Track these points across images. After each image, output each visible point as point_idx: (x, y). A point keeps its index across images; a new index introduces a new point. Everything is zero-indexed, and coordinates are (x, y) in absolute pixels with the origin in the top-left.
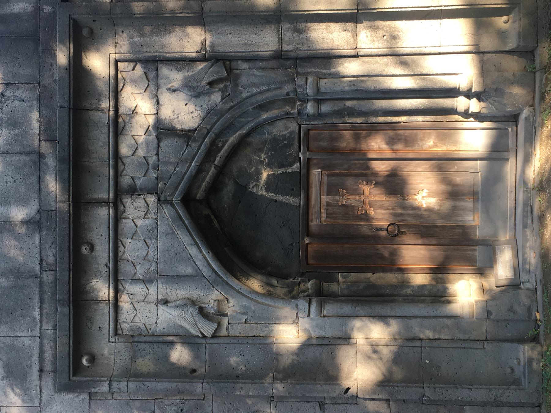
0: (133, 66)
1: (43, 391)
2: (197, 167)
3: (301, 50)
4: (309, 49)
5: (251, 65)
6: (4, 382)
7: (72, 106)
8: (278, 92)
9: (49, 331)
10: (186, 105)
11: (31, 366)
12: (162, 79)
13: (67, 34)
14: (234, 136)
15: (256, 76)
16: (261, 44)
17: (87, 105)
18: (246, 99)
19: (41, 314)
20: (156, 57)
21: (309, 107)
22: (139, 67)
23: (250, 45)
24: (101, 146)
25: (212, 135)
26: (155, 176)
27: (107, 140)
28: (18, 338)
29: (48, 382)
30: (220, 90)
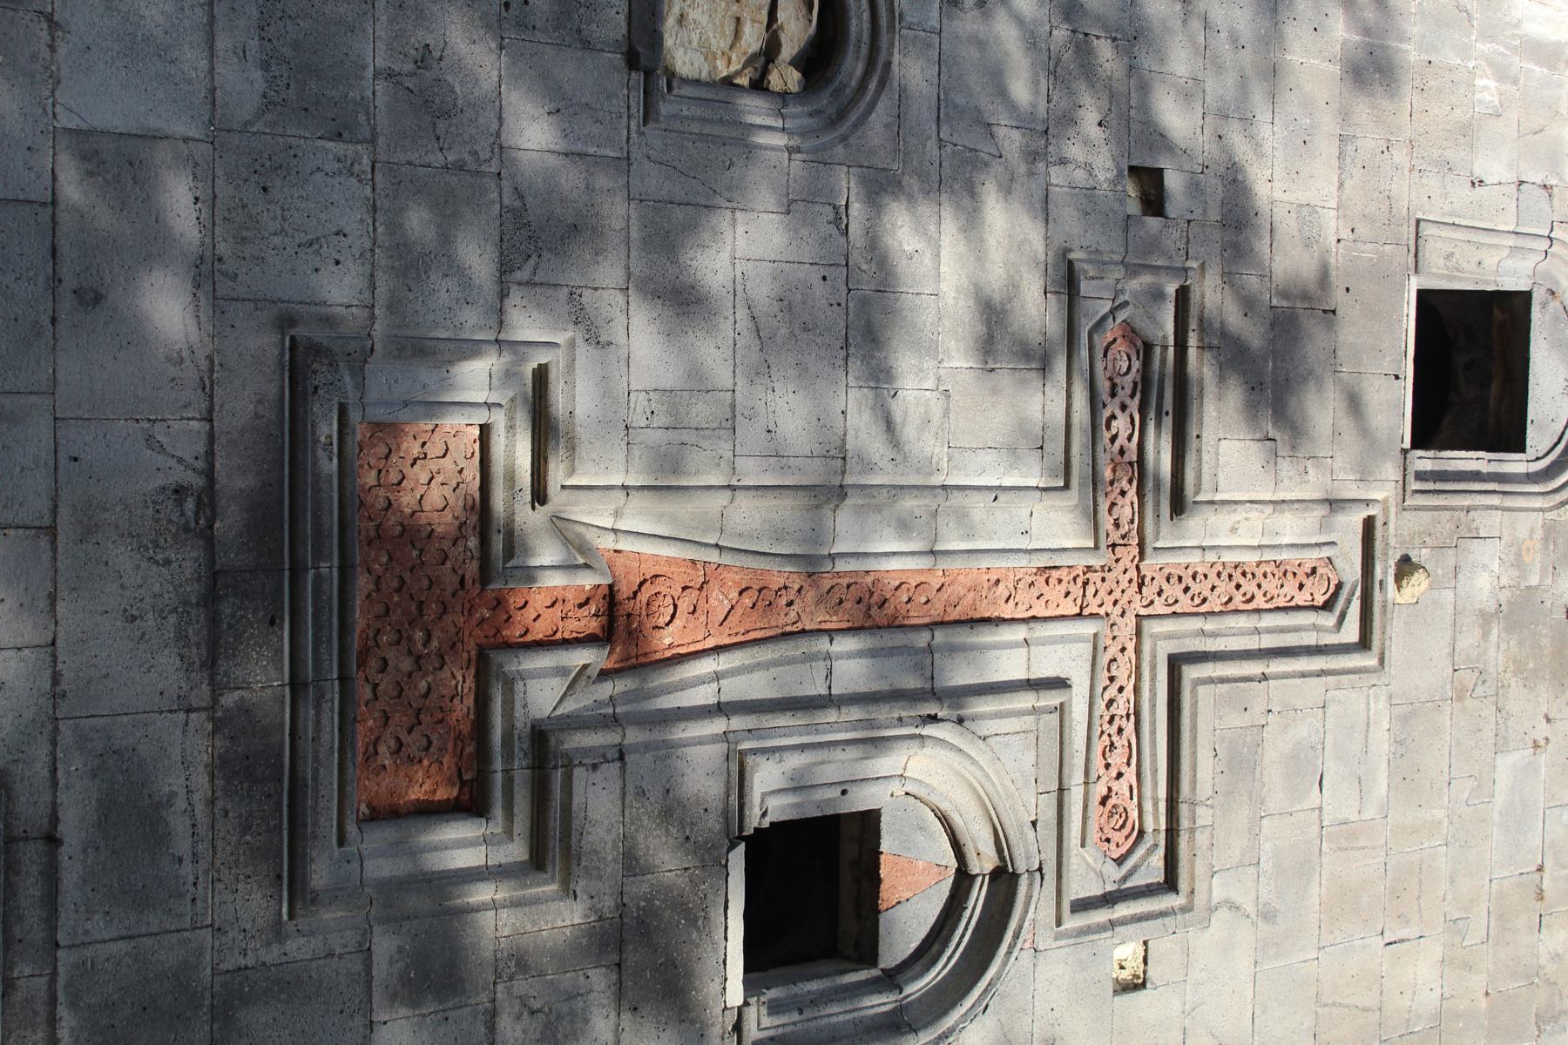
1: (45, 773)
6: (167, 789)
9: (27, 971)
11: (84, 851)
19: (52, 1021)
28: (124, 933)
29: (29, 807)
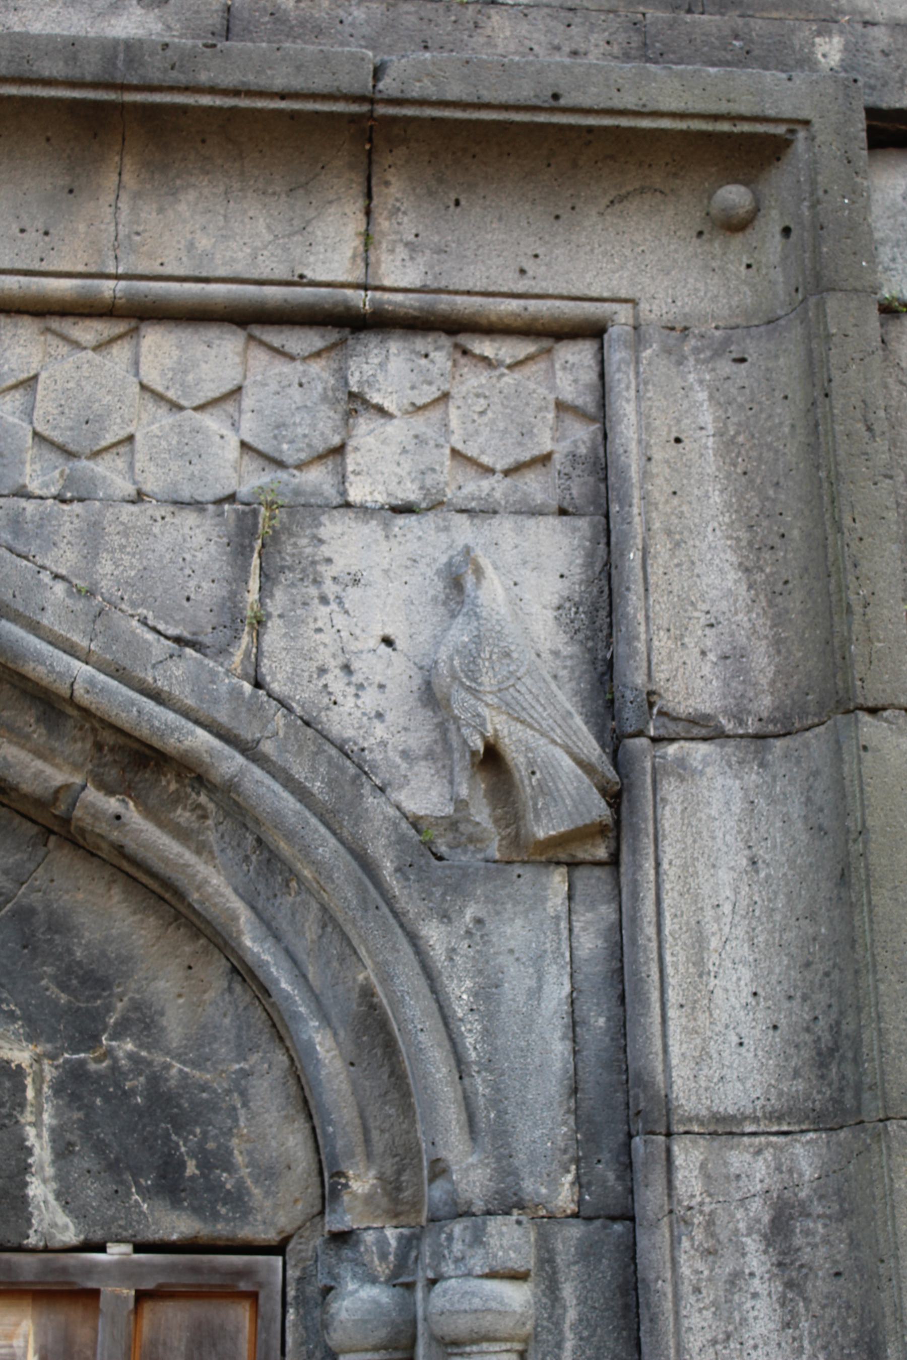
0: (579, 402)
2: (64, 691)
3: (675, 1242)
4: (686, 1288)
5: (594, 970)
7: (382, 110)
8: (451, 1115)
10: (388, 641)
12: (519, 531)
13: (723, 107)
14: (228, 892)
15: (536, 993)
16: (702, 1017)
17: (394, 190)
18: (413, 939)
20: (626, 502)
21: (369, 1292)
22: (581, 434)
23: (699, 963)
24: (191, 246)
25: (230, 763)
26: (34, 487)
27: (221, 272)
30: (460, 804)
